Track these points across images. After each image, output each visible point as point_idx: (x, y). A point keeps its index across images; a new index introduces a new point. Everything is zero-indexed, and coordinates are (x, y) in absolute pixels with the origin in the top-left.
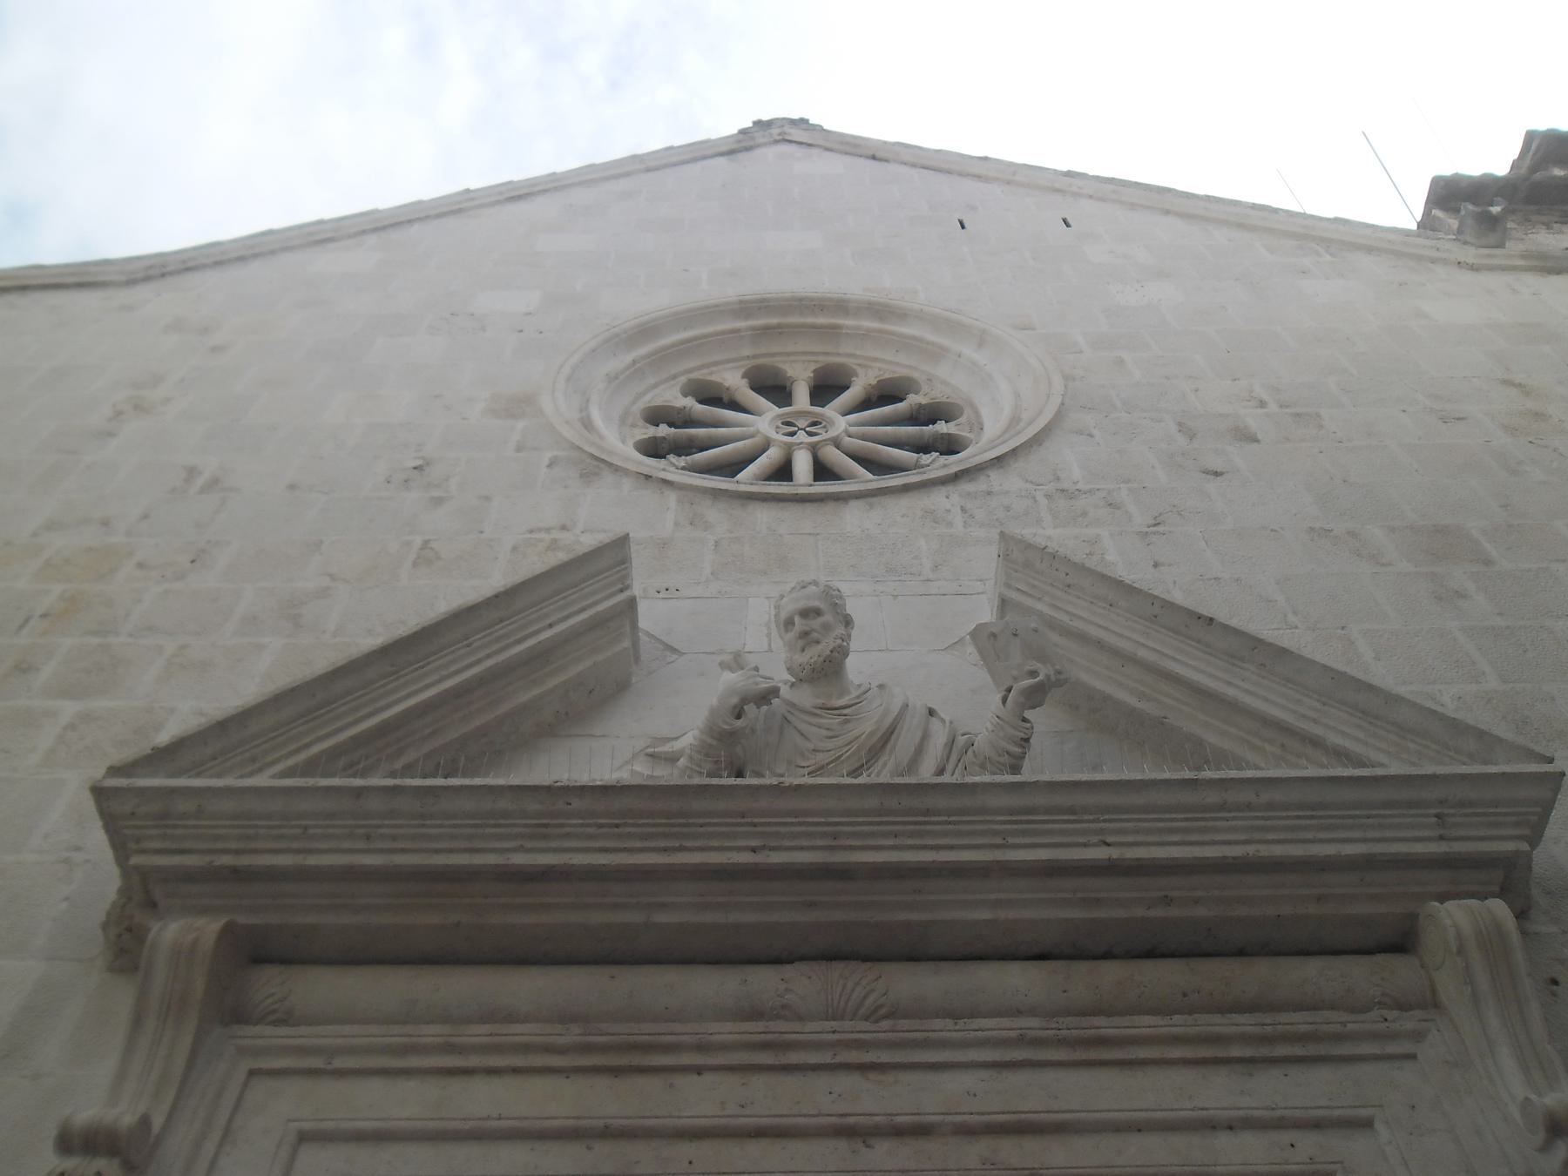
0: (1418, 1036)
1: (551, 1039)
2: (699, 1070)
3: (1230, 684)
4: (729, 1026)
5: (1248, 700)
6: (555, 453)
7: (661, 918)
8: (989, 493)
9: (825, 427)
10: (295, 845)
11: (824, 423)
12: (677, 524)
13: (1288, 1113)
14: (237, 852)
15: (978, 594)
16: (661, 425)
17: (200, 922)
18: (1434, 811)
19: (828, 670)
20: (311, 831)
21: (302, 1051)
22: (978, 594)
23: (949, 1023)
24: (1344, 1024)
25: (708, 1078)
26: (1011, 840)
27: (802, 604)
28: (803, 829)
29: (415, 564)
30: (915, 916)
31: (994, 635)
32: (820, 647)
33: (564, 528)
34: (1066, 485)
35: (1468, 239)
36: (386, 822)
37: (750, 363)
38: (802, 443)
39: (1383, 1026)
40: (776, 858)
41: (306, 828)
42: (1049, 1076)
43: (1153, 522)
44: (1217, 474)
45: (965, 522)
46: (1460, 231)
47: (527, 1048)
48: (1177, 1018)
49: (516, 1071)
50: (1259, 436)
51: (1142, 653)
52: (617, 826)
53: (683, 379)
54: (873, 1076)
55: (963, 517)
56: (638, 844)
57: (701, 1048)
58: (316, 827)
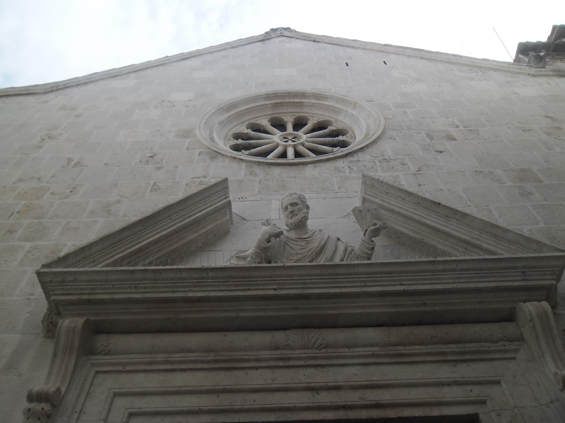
0: (517, 351)
1: (204, 358)
2: (257, 368)
3: (446, 226)
4: (268, 352)
5: (454, 232)
6: (201, 150)
7: (242, 314)
8: (358, 161)
9: (298, 139)
10: (110, 291)
11: (298, 137)
13: (469, 379)
14: (89, 294)
15: (355, 197)
16: (239, 140)
17: (76, 319)
19: (301, 225)
20: (116, 286)
21: (114, 364)
22: (355, 197)
23: (346, 350)
24: (489, 347)
25: (260, 371)
26: (368, 284)
27: (291, 201)
28: (292, 281)
29: (151, 191)
30: (334, 312)
31: (360, 211)
32: (297, 217)
33: (204, 177)
34: (386, 157)
35: (532, 65)
36: (143, 282)
37: (271, 117)
38: (290, 145)
39: (503, 348)
40: (283, 292)
41: (114, 285)
42: (383, 368)
43: (418, 170)
44: (441, 152)
45: (350, 171)
46: (529, 62)
47: (195, 362)
48: (429, 347)
49: (191, 370)
50: (456, 138)
51: (415, 217)
52: (226, 282)
53: (247, 123)
54: (320, 369)
55: (349, 170)
56: (233, 288)
57: (257, 360)
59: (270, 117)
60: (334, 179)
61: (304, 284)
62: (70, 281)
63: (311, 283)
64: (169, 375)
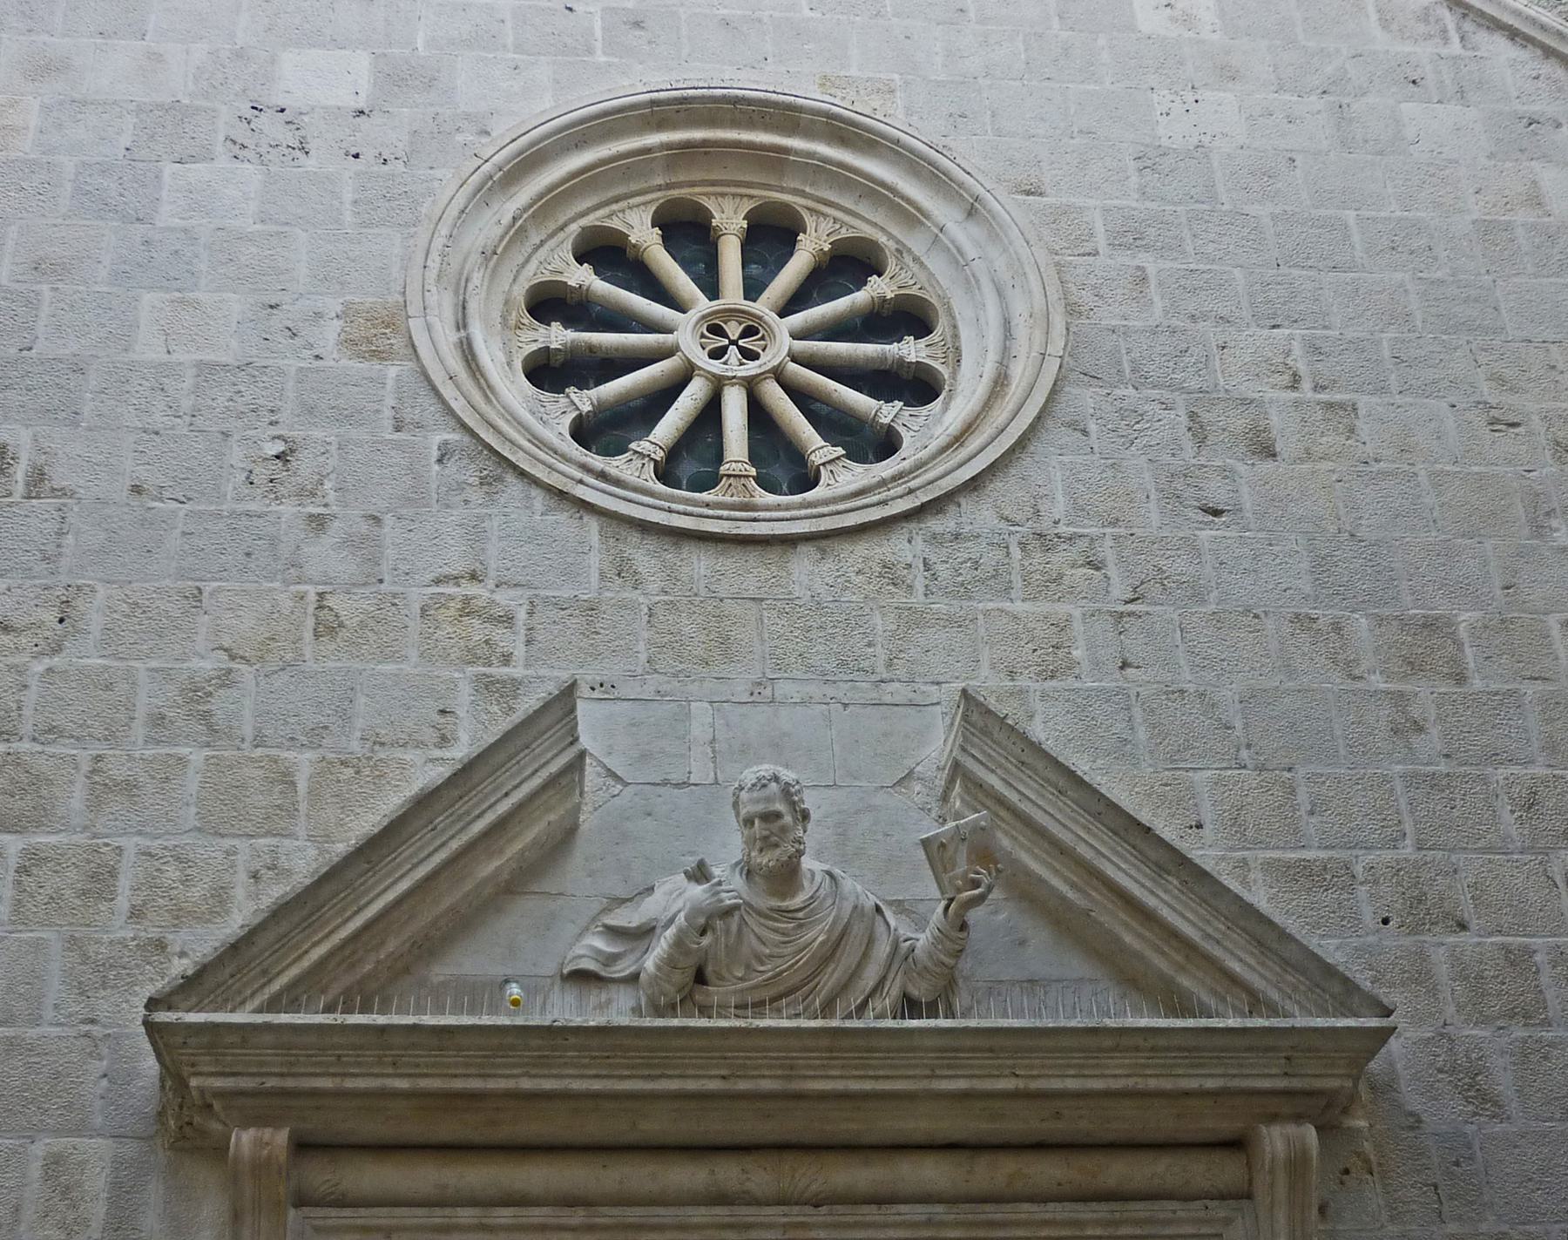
0: (1227, 1222)
3: (1152, 892)
4: (703, 1210)
5: (1165, 912)
6: (447, 436)
8: (957, 536)
9: (763, 338)
11: (762, 332)
12: (602, 576)
14: (282, 1075)
15: (932, 704)
17: (267, 1133)
18: (1284, 1054)
19: (786, 876)
22: (932, 704)
23: (874, 1208)
24: (1174, 1212)
26: (938, 1072)
27: (760, 808)
29: (317, 635)
31: (943, 845)
32: (778, 852)
33: (473, 577)
34: (1045, 525)
38: (734, 377)
40: (743, 1085)
41: (339, 1056)
43: (1130, 596)
44: (1217, 513)
45: (926, 586)
48: (1051, 1206)
51: (1082, 849)
53: (574, 228)
58: (348, 1055)
59: (658, 199)
60: (877, 619)
61: (791, 1067)
62: (232, 1045)
63: (810, 1067)
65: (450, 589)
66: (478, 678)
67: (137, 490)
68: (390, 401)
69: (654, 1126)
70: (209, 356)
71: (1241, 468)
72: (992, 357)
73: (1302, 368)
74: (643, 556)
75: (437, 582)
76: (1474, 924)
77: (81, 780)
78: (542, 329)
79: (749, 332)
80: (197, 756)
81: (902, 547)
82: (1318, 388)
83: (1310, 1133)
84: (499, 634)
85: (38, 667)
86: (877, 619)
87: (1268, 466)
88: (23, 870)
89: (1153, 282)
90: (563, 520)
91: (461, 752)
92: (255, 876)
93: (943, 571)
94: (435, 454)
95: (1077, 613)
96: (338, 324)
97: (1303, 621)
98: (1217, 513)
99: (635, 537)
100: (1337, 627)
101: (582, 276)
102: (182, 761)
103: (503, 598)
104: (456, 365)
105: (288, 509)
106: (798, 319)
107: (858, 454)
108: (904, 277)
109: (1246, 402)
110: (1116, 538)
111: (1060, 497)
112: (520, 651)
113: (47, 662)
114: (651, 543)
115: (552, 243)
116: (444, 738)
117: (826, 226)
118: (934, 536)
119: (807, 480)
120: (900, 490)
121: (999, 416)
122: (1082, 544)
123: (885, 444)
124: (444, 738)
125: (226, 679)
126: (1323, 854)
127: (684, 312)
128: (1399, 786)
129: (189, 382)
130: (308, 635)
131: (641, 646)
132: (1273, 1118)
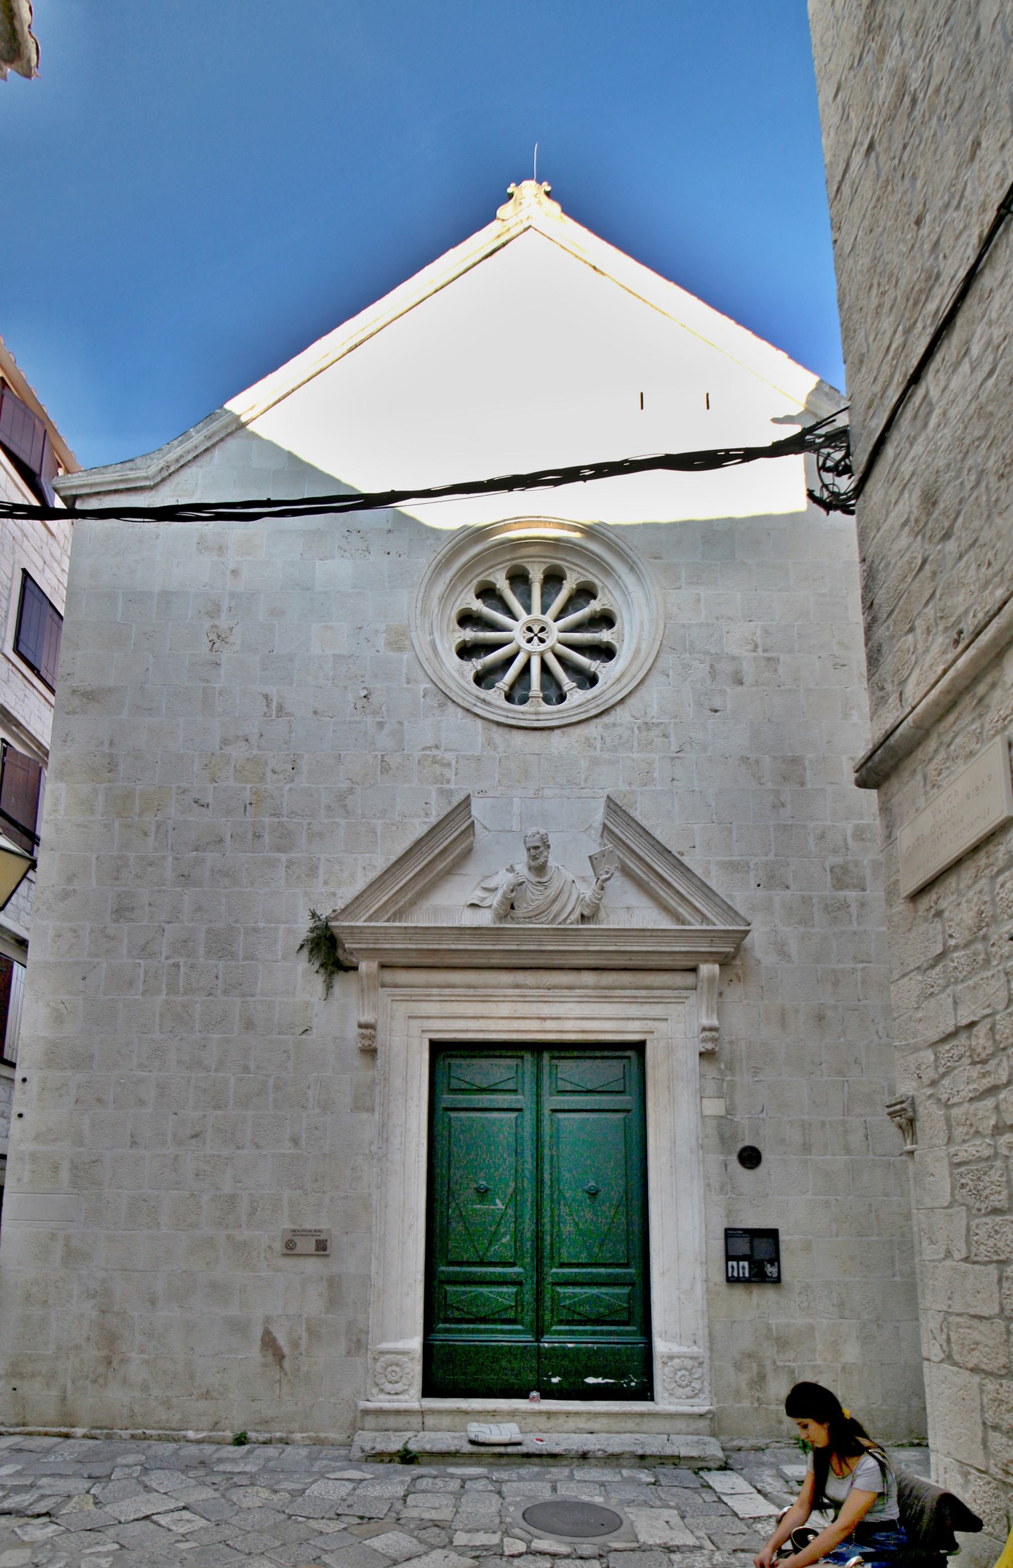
8: (614, 725)
12: (483, 745)
21: (403, 995)
29: (382, 773)
33: (437, 747)
34: (648, 720)
44: (716, 711)
47: (459, 996)
53: (475, 582)
57: (505, 996)
64: (444, 1004)
65: (428, 753)
66: (439, 788)
67: (315, 712)
68: (405, 670)
69: (495, 961)
70: (337, 652)
71: (728, 689)
72: (635, 640)
73: (759, 641)
74: (499, 735)
75: (424, 749)
76: (792, 887)
77: (304, 832)
78: (463, 632)
79: (543, 629)
80: (343, 822)
81: (592, 730)
82: (765, 650)
83: (717, 967)
84: (446, 771)
85: (287, 787)
86: (582, 762)
87: (740, 688)
88: (287, 867)
89: (702, 601)
90: (469, 721)
91: (434, 820)
92: (364, 868)
93: (608, 740)
94: (422, 694)
95: (657, 758)
96: (384, 635)
97: (745, 759)
98: (716, 711)
99: (494, 728)
100: (757, 762)
101: (478, 606)
102: (338, 824)
103: (450, 756)
104: (429, 652)
105: (369, 719)
106: (561, 623)
107: (581, 686)
108: (605, 601)
109: (734, 658)
110: (675, 724)
111: (655, 706)
112: (453, 778)
113: (289, 786)
114: (501, 730)
115: (466, 590)
116: (427, 814)
117: (575, 576)
118: (606, 725)
119: (562, 698)
120: (594, 705)
121: (634, 669)
122: (662, 727)
123: (592, 680)
124: (427, 814)
125: (351, 791)
126: (739, 858)
127: (517, 620)
128: (772, 829)
129: (331, 665)
130: (379, 773)
131: (496, 775)
132: (706, 961)
